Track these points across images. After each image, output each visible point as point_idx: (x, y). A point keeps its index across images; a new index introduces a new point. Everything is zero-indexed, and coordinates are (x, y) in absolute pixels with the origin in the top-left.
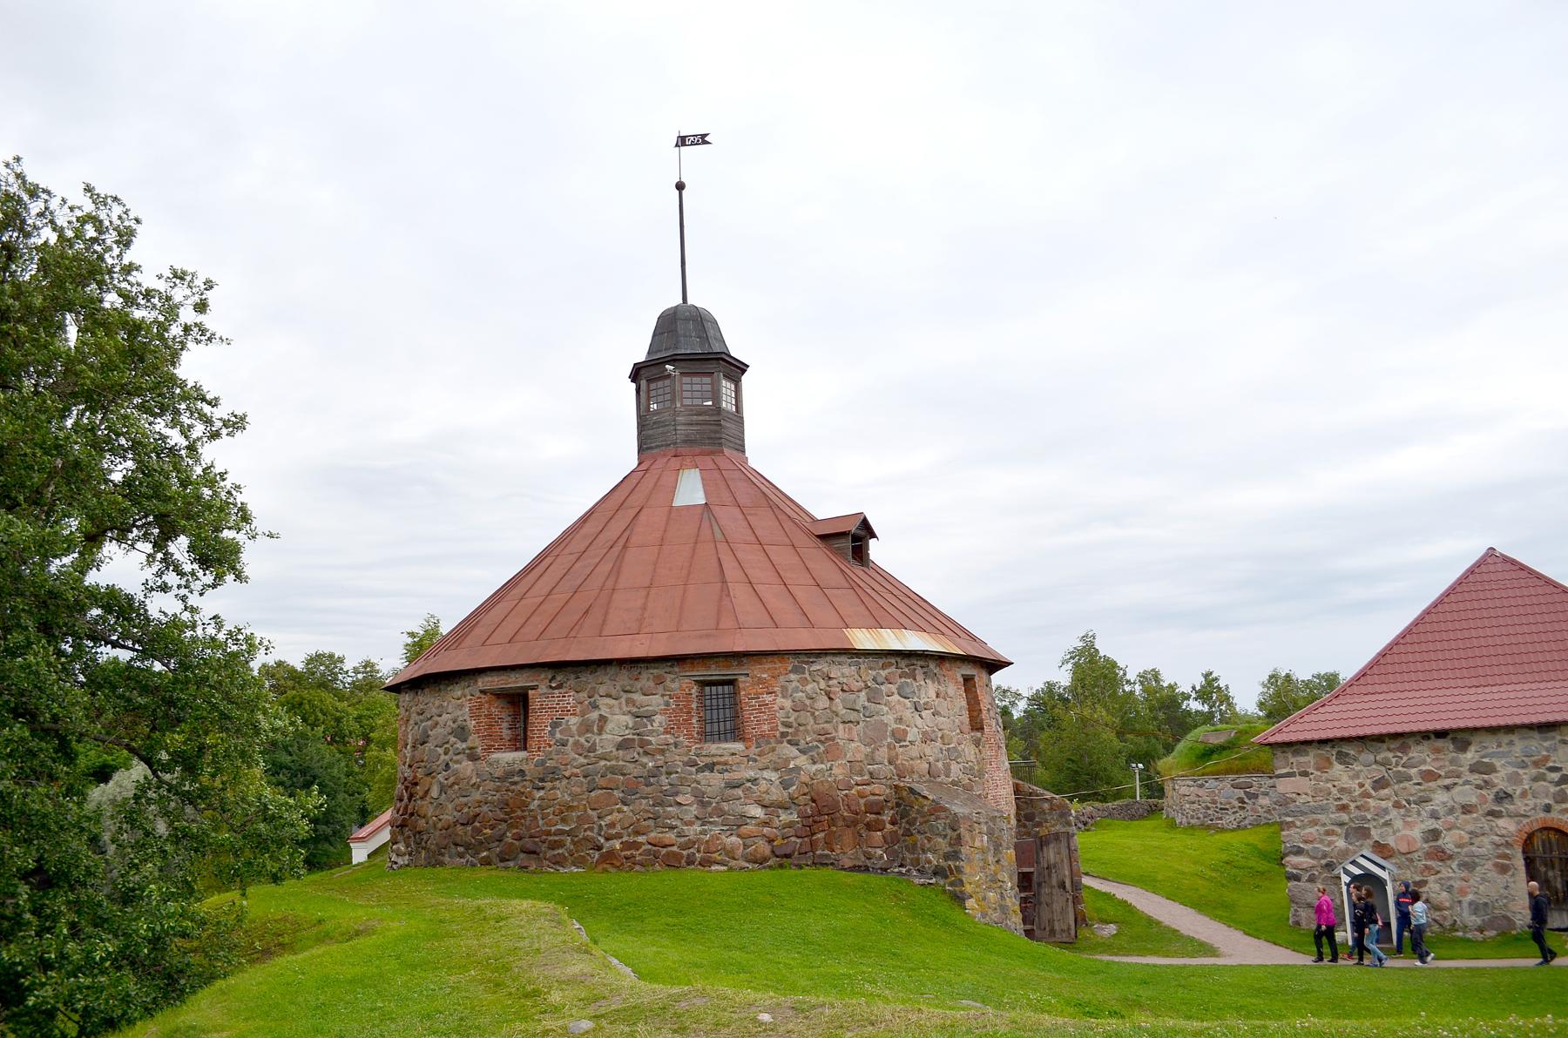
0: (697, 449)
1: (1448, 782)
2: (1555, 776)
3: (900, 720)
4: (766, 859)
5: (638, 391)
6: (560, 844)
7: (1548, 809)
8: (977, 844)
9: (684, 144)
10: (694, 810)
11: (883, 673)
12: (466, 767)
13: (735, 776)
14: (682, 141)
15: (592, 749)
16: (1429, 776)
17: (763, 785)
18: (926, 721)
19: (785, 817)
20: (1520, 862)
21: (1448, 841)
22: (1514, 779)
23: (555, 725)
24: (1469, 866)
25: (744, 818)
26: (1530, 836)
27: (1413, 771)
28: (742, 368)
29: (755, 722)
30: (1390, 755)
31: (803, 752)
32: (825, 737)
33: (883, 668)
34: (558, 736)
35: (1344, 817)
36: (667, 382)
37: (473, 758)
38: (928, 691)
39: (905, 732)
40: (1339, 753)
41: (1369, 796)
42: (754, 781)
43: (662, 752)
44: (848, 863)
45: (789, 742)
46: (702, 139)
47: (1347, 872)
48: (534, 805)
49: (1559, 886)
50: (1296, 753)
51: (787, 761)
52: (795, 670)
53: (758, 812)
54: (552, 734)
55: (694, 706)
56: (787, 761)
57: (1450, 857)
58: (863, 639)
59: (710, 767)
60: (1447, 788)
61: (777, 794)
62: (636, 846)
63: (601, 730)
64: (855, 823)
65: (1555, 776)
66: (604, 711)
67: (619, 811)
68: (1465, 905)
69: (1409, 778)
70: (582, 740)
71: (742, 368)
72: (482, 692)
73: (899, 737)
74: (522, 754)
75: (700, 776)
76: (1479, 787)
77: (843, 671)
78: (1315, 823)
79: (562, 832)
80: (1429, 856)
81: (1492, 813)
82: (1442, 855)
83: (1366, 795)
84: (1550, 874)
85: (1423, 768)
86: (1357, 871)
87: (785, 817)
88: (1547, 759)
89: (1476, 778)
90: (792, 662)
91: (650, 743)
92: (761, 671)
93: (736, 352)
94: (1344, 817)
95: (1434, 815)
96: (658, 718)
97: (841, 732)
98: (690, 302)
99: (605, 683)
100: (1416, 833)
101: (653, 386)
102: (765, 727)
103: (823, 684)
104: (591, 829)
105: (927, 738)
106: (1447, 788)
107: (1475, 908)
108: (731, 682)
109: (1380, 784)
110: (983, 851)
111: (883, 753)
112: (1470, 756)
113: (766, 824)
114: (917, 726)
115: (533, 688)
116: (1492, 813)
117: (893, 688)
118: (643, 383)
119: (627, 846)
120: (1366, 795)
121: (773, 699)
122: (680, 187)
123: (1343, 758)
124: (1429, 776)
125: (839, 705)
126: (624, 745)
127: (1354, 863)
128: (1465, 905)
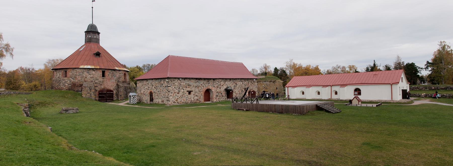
18: (92, 76)
29: (68, 75)
32: (75, 77)
38: (94, 72)
58: (82, 67)
73: (86, 77)
92: (69, 70)
97: (78, 77)
99: (58, 71)
111: (83, 79)
114: (89, 76)
121: (70, 73)
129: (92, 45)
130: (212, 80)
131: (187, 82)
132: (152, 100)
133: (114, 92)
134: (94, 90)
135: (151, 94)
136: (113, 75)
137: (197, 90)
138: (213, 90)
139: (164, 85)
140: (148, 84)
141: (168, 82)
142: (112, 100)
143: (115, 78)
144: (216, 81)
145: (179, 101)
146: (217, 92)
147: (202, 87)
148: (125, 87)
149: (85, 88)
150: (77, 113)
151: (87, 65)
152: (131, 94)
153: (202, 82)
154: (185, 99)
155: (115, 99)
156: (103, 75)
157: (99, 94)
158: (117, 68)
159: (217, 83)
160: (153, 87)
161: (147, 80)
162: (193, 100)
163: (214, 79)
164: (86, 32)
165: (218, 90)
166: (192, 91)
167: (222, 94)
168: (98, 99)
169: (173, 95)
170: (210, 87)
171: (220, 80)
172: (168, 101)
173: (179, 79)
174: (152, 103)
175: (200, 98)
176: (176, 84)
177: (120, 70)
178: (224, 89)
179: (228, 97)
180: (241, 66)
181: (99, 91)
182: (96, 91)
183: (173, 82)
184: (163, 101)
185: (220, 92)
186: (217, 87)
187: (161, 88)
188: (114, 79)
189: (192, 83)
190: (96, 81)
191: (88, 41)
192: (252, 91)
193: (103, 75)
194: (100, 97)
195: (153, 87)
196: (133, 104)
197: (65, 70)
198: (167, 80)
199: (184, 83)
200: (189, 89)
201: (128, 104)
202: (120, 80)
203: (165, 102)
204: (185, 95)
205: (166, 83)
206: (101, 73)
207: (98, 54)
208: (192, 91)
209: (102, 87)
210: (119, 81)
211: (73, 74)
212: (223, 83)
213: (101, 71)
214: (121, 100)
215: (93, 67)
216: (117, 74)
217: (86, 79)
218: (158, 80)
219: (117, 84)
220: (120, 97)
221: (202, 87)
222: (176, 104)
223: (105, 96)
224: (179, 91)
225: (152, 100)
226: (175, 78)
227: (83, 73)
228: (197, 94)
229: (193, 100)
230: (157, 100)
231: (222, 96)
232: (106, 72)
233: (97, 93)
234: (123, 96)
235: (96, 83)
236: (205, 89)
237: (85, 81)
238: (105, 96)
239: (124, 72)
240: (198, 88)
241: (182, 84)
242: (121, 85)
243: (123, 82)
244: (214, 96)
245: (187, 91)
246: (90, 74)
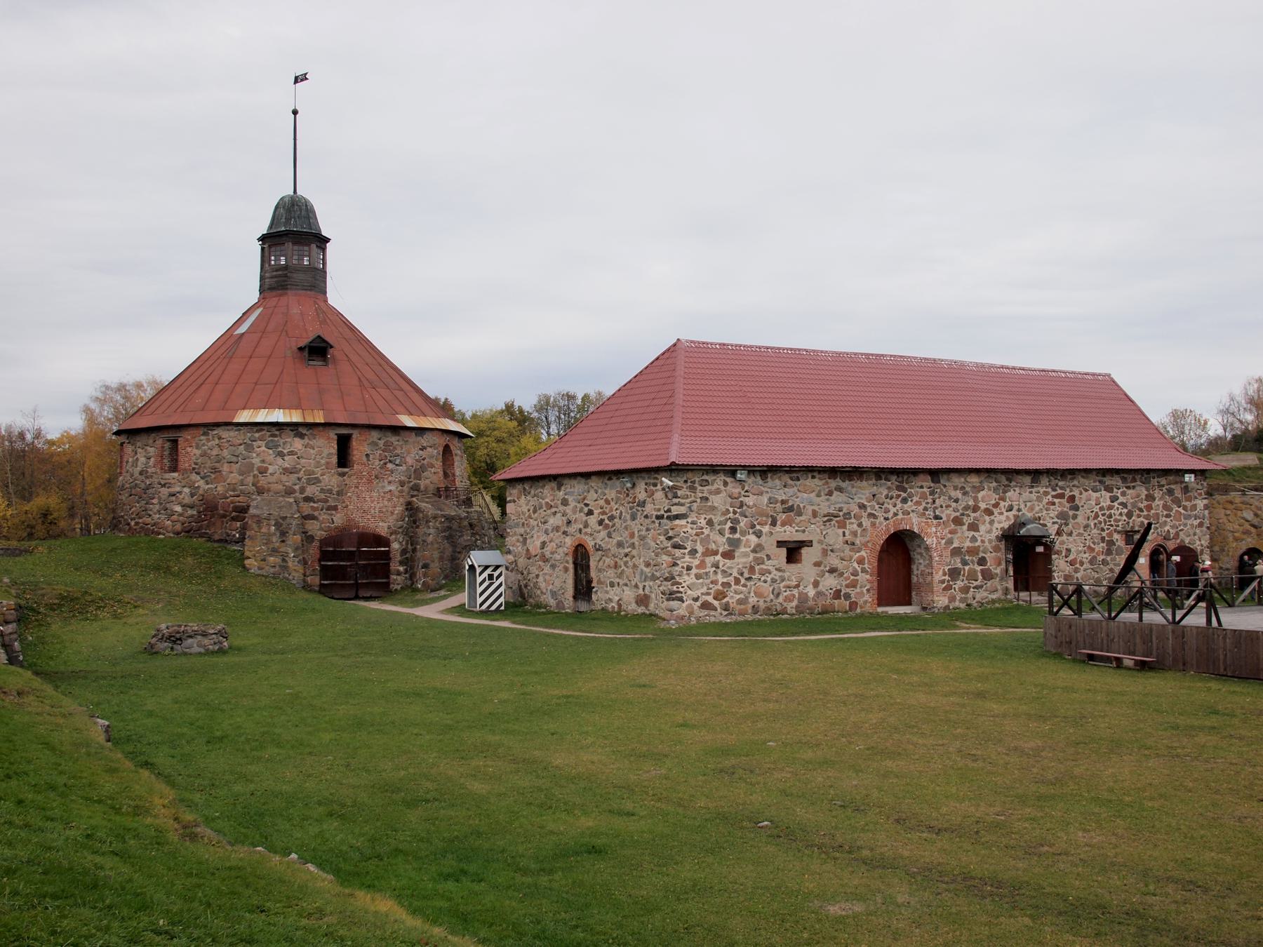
0: (274, 293)
1: (553, 510)
3: (263, 461)
4: (178, 533)
8: (264, 530)
10: (157, 507)
11: (257, 435)
13: (172, 490)
18: (288, 462)
19: (190, 512)
20: (571, 566)
21: (547, 551)
24: (553, 566)
29: (184, 463)
32: (215, 470)
33: (257, 431)
38: (298, 444)
39: (267, 469)
42: (180, 493)
44: (216, 537)
52: (205, 434)
53: (178, 509)
55: (166, 453)
58: (244, 416)
59: (164, 486)
61: (187, 500)
64: (224, 516)
65: (586, 509)
73: (263, 471)
78: (515, 534)
82: (545, 560)
87: (190, 512)
89: (561, 508)
90: (201, 430)
92: (186, 436)
95: (546, 532)
97: (225, 468)
98: (299, 192)
99: (141, 440)
100: (538, 544)
103: (217, 441)
107: (554, 594)
109: (535, 512)
110: (270, 535)
111: (250, 479)
113: (181, 515)
114: (276, 466)
116: (565, 533)
117: (263, 443)
119: (137, 524)
121: (191, 451)
122: (295, 112)
125: (225, 453)
126: (141, 473)
129: (294, 304)
130: (926, 482)
131: (777, 489)
132: (583, 589)
133: (395, 546)
134: (298, 537)
135: (581, 557)
136: (389, 457)
137: (835, 536)
138: (933, 536)
139: (649, 508)
140: (565, 502)
141: (672, 492)
142: (383, 590)
143: (400, 473)
144: (951, 488)
145: (732, 599)
146: (956, 552)
147: (866, 522)
148: (449, 519)
149: (259, 522)
150: (221, 651)
151: (268, 405)
152: (477, 558)
153: (863, 491)
154: (767, 589)
155: (397, 581)
156: (344, 459)
157: (324, 555)
158: (408, 421)
159: (952, 496)
160: (593, 520)
161: (557, 479)
162: (811, 592)
163: (935, 474)
164: (263, 239)
165: (963, 538)
166: (809, 544)
167: (982, 561)
168: (315, 580)
169: (702, 565)
170: (914, 523)
171: (974, 479)
172: (671, 596)
173: (731, 471)
174: (583, 606)
175: (853, 585)
176: (718, 501)
177: (420, 431)
178: (996, 532)
179: (1023, 582)
180: (1101, 398)
181: (324, 542)
182: (309, 539)
183: (703, 491)
184: (643, 600)
185: (973, 551)
186: (958, 521)
187: (635, 526)
188: (396, 477)
189: (808, 494)
190: (310, 490)
191: (276, 282)
192: (1171, 545)
193: (344, 459)
194: (325, 572)
195: (593, 520)
196: (486, 613)
197: (172, 435)
198: (667, 482)
199: (761, 496)
200: (790, 533)
201: (460, 610)
202: (422, 484)
203: (658, 605)
204: (768, 565)
205: (659, 495)
206: (333, 448)
207: (318, 350)
208: (809, 544)
209: (339, 519)
210: (416, 488)
211: (204, 454)
212: (994, 498)
213: (333, 434)
214: (428, 588)
215: (296, 417)
216: (411, 452)
217: (263, 481)
218: (617, 483)
219: (410, 507)
220: (420, 572)
221: (866, 522)
222: (718, 616)
223: (354, 567)
224: (735, 544)
225: (583, 589)
226: (713, 469)
227: (249, 448)
228: (833, 561)
229: (811, 592)
230: (614, 594)
231: (987, 575)
232: (354, 443)
233: (314, 551)
234: (435, 567)
235: (307, 499)
236: (884, 529)
237: (260, 491)
238: (354, 567)
239: (441, 441)
240: (842, 525)
241: (750, 501)
242: (426, 506)
243: (438, 493)
244: (938, 576)
245: (780, 544)
246: (281, 455)
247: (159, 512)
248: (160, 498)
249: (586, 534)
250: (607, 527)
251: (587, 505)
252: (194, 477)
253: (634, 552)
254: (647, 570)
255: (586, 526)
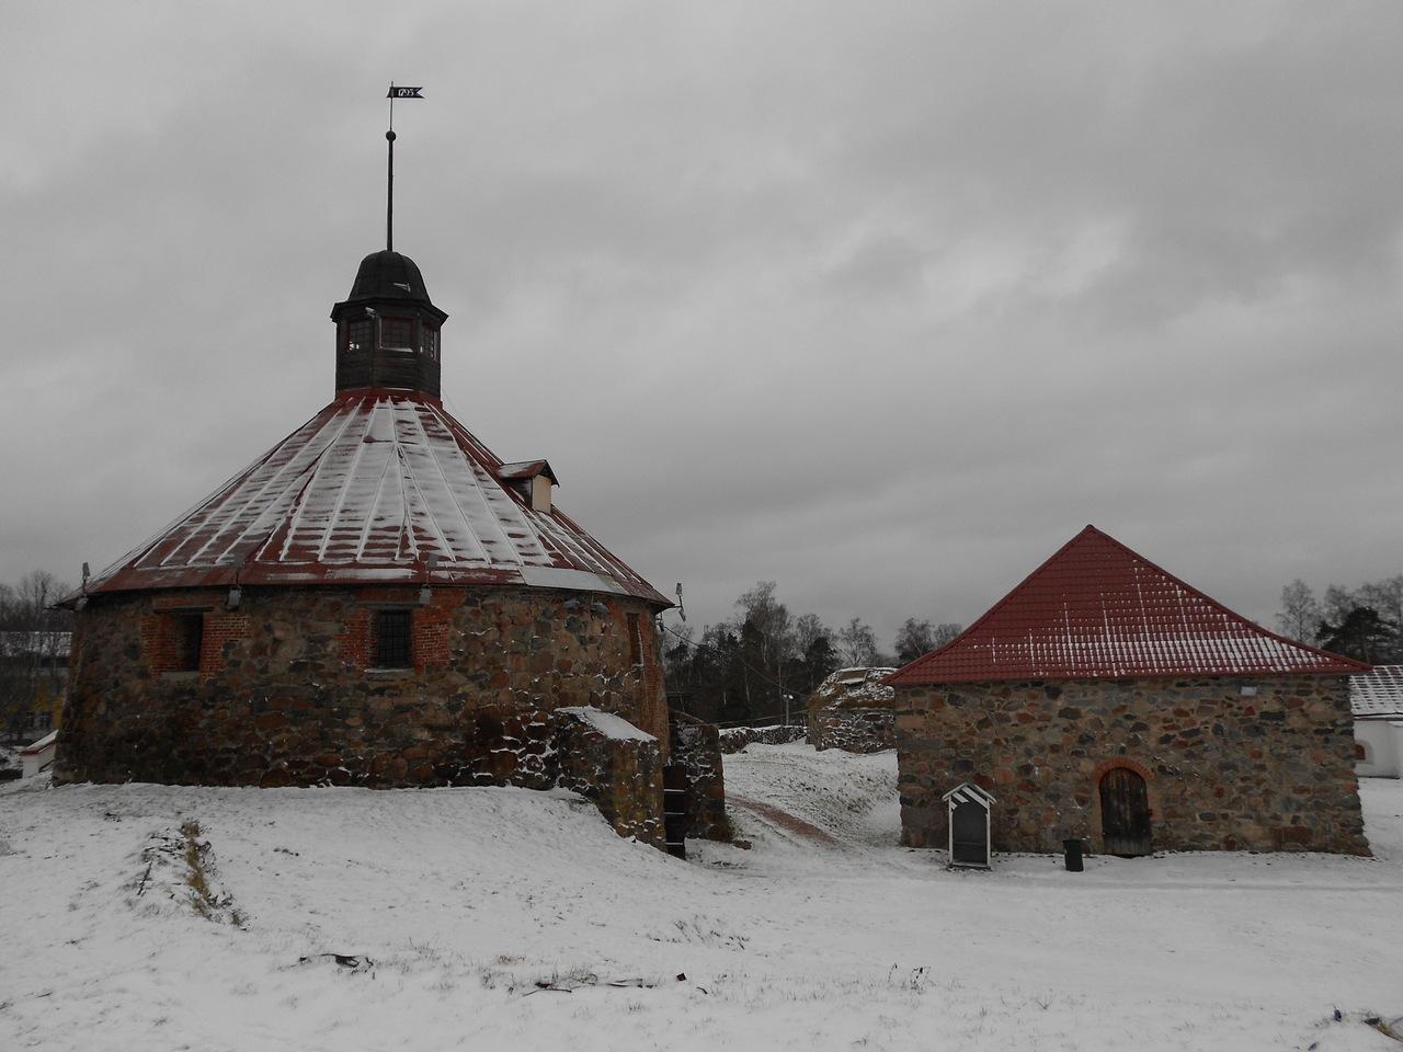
1: (1040, 724)
2: (1130, 724)
5: (338, 329)
6: (228, 761)
7: (1122, 750)
9: (396, 96)
12: (136, 686)
13: (405, 700)
14: (394, 92)
15: (264, 670)
16: (1025, 718)
17: (431, 712)
20: (1096, 795)
22: (1098, 724)
23: (229, 645)
25: (409, 742)
26: (1107, 774)
27: (1011, 714)
28: (443, 317)
30: (994, 699)
31: (472, 679)
34: (231, 657)
35: (953, 752)
36: (367, 324)
37: (144, 675)
40: (951, 696)
41: (974, 733)
42: (423, 706)
43: (334, 676)
45: (459, 670)
46: (414, 93)
47: (954, 800)
48: (202, 723)
49: (1128, 818)
50: (915, 694)
51: (456, 687)
53: (425, 735)
54: (225, 655)
55: (369, 632)
56: (456, 687)
57: (1039, 790)
59: (381, 691)
60: (1040, 729)
61: (442, 719)
62: (301, 764)
63: (274, 652)
65: (1130, 724)
66: (278, 634)
67: (288, 731)
68: (1049, 831)
69: (1008, 720)
70: (255, 662)
71: (443, 317)
72: (157, 612)
73: (565, 667)
74: (190, 676)
75: (371, 699)
76: (1065, 730)
77: (512, 607)
79: (229, 751)
80: (1020, 787)
81: (1076, 753)
82: (1030, 786)
83: (972, 733)
84: (1122, 807)
85: (1021, 711)
86: (963, 800)
88: (1124, 707)
89: (1064, 722)
91: (322, 666)
93: (437, 300)
94: (953, 752)
95: (1029, 753)
96: (332, 646)
97: (508, 665)
101: (353, 327)
102: (437, 655)
104: (258, 748)
105: (592, 668)
106: (1040, 729)
108: (407, 613)
112: (1060, 703)
115: (210, 610)
116: (1076, 753)
118: (344, 322)
119: (292, 765)
120: (972, 733)
122: (391, 136)
123: (954, 700)
124: (1025, 718)
126: (297, 667)
127: (960, 792)
128: (1049, 831)
139: (1295, 721)
227: (543, 629)
247: (369, 740)
248: (368, 719)
249: (1140, 754)
250: (1183, 745)
251: (1128, 717)
252: (456, 678)
253: (1265, 775)
254: (1295, 796)
255: (1135, 742)
